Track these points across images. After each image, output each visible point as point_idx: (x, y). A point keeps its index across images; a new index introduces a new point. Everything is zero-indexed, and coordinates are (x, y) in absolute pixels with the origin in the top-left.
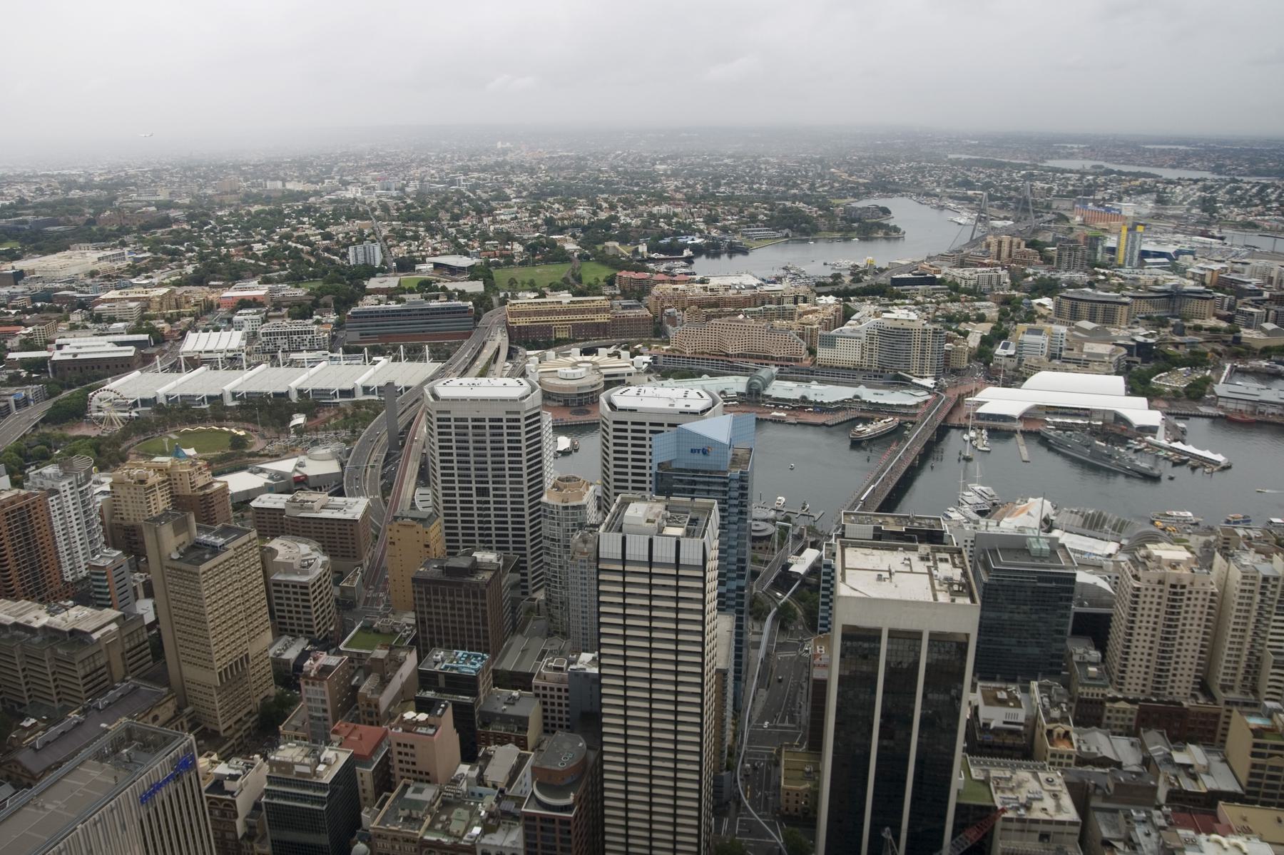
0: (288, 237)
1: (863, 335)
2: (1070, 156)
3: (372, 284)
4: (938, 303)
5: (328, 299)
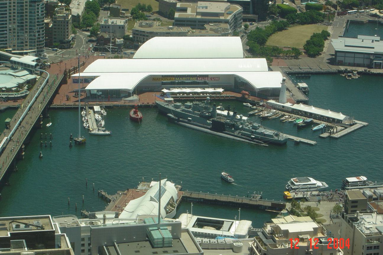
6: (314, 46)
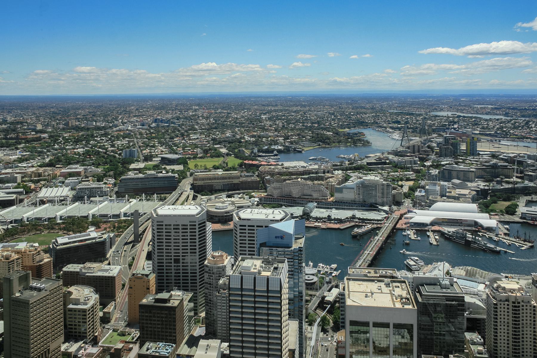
0: (95, 146)
1: (355, 187)
2: (441, 110)
3: (132, 166)
4: (388, 173)
5: (112, 173)
6: (511, 211)
